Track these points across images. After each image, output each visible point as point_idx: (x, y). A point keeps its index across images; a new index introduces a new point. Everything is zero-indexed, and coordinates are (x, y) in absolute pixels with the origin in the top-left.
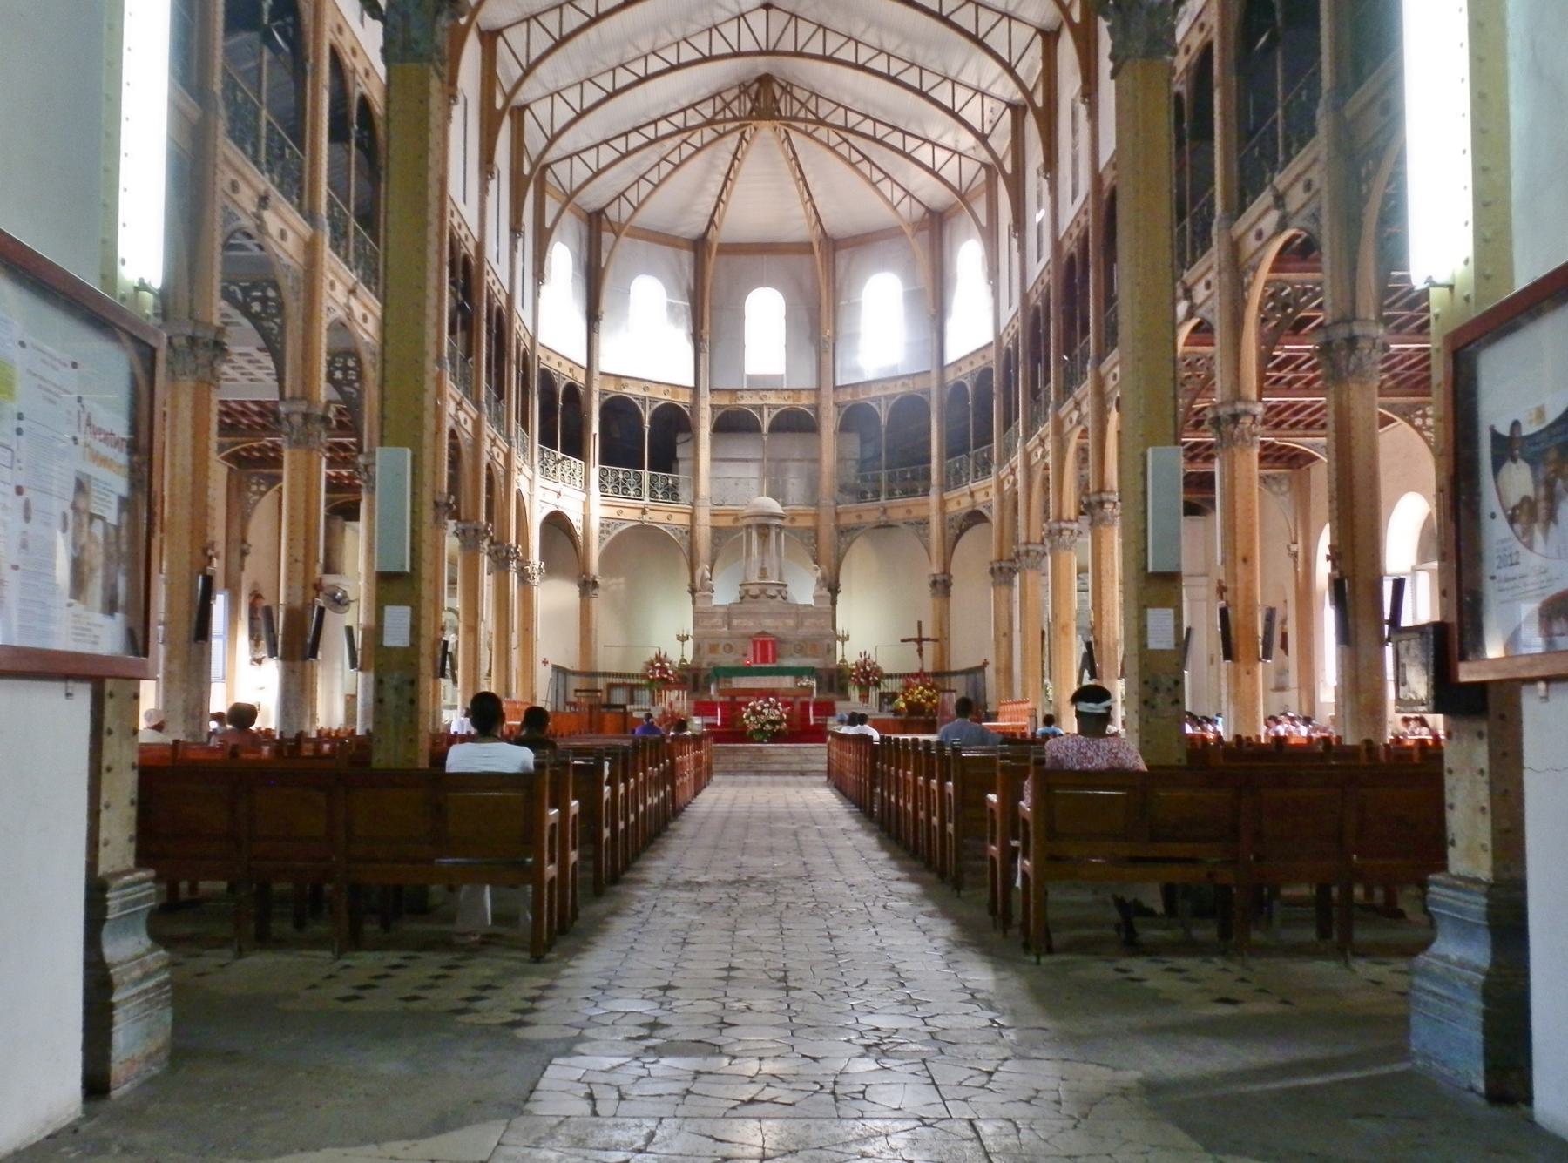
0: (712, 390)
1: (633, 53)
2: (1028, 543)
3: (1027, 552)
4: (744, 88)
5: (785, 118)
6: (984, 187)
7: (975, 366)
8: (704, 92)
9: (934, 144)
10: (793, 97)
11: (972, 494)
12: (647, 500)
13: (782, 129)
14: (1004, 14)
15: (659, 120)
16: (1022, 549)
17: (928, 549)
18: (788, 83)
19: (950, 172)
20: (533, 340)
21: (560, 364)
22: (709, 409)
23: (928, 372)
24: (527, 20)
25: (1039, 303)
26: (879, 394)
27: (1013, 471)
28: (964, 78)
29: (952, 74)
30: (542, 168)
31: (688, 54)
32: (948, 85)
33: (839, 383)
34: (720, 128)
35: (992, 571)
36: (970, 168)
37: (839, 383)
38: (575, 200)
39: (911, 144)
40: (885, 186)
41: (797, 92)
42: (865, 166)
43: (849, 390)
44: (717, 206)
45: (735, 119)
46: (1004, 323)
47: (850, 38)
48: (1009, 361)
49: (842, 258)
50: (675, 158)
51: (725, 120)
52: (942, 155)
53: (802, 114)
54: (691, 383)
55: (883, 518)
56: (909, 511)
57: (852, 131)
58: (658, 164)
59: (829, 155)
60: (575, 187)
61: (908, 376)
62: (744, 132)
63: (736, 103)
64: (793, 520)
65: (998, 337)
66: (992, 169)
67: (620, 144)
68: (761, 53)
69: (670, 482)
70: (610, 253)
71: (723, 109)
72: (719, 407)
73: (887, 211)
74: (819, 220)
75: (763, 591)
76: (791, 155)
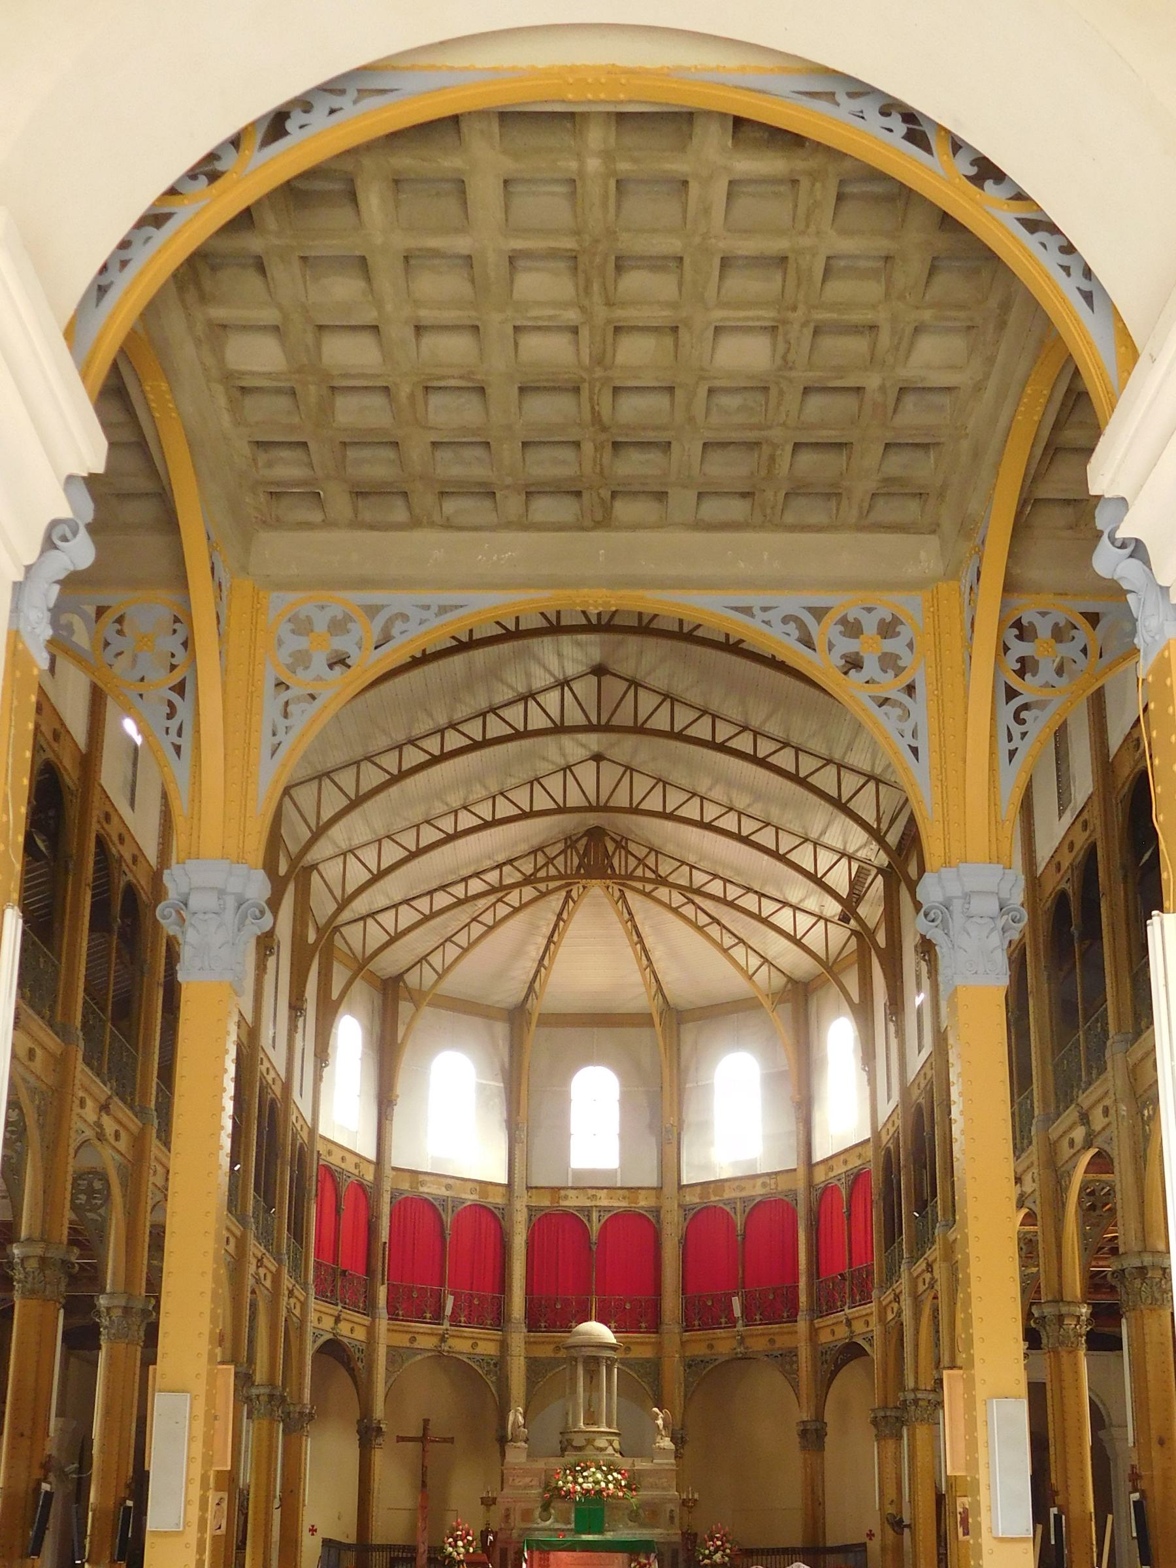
0: (529, 1188)
1: (440, 808)
2: (916, 1390)
3: (916, 1401)
4: (570, 842)
5: (620, 877)
6: (855, 955)
7: (850, 1166)
8: (524, 848)
9: (795, 908)
10: (629, 852)
11: (849, 1323)
13: (616, 887)
14: (870, 777)
15: (470, 877)
16: (910, 1396)
17: (795, 1388)
18: (623, 837)
19: (815, 940)
20: (313, 1131)
21: (343, 1159)
22: (525, 1210)
23: (795, 1170)
24: (319, 777)
25: (921, 1100)
26: (734, 1195)
27: (897, 1298)
28: (827, 839)
29: (813, 835)
30: (331, 929)
31: (504, 809)
32: (809, 847)
33: (685, 1182)
34: (542, 887)
35: (875, 1422)
36: (839, 934)
37: (685, 1182)
38: (371, 966)
39: (768, 907)
40: (739, 953)
41: (632, 847)
42: (714, 930)
43: (698, 1189)
44: (537, 972)
45: (560, 877)
46: (882, 1117)
47: (694, 794)
48: (889, 1164)
49: (688, 1034)
50: (488, 918)
51: (548, 878)
52: (804, 921)
53: (639, 872)
54: (504, 1181)
55: (740, 1349)
57: (698, 892)
58: (468, 925)
59: (670, 916)
60: (369, 952)
61: (768, 1174)
62: (569, 892)
63: (562, 858)
64: (628, 1349)
65: (876, 1134)
66: (863, 936)
67: (423, 905)
68: (590, 808)
69: (476, 1302)
70: (409, 1027)
71: (546, 865)
72: (540, 1209)
73: (740, 979)
74: (660, 988)
75: (590, 1442)
76: (626, 916)
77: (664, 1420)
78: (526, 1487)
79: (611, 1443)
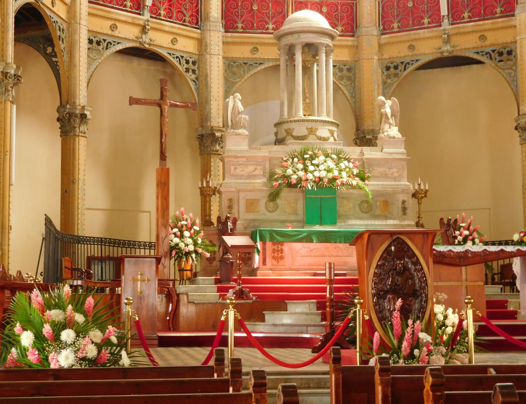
12: (147, 15)
56: (483, 38)
75: (312, 131)
77: (391, 107)
78: (250, 176)
79: (332, 132)
